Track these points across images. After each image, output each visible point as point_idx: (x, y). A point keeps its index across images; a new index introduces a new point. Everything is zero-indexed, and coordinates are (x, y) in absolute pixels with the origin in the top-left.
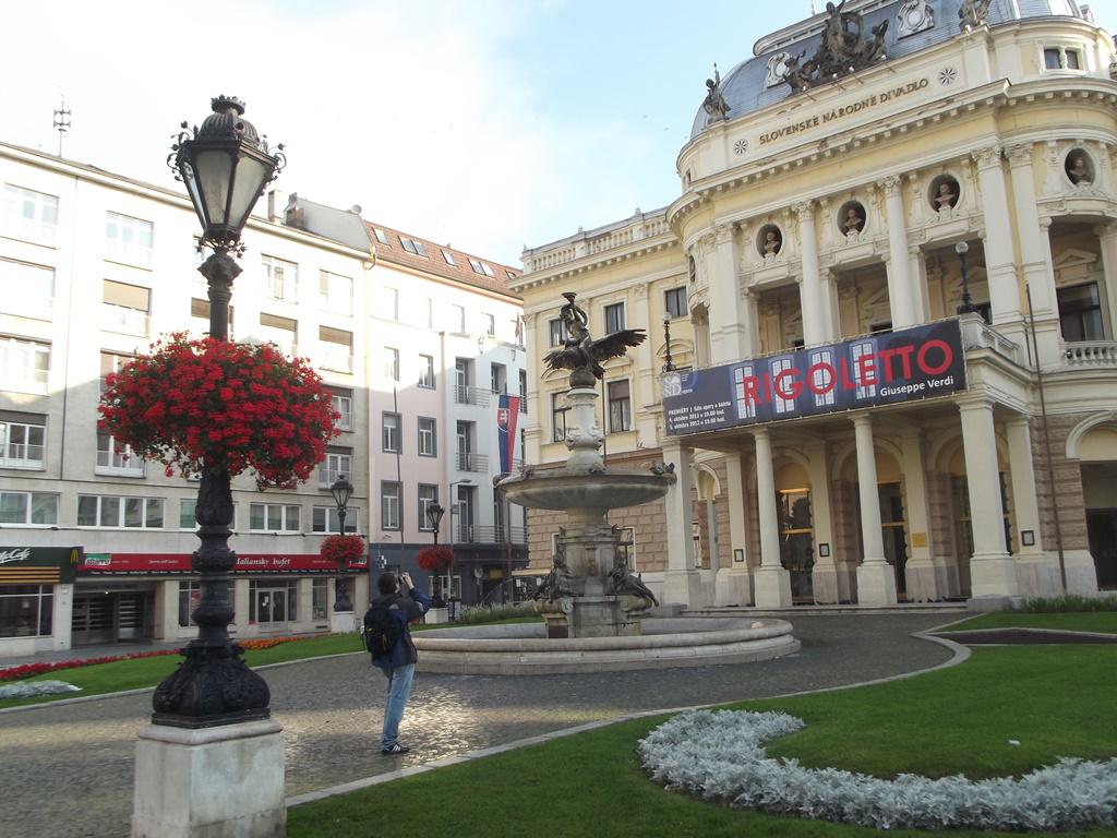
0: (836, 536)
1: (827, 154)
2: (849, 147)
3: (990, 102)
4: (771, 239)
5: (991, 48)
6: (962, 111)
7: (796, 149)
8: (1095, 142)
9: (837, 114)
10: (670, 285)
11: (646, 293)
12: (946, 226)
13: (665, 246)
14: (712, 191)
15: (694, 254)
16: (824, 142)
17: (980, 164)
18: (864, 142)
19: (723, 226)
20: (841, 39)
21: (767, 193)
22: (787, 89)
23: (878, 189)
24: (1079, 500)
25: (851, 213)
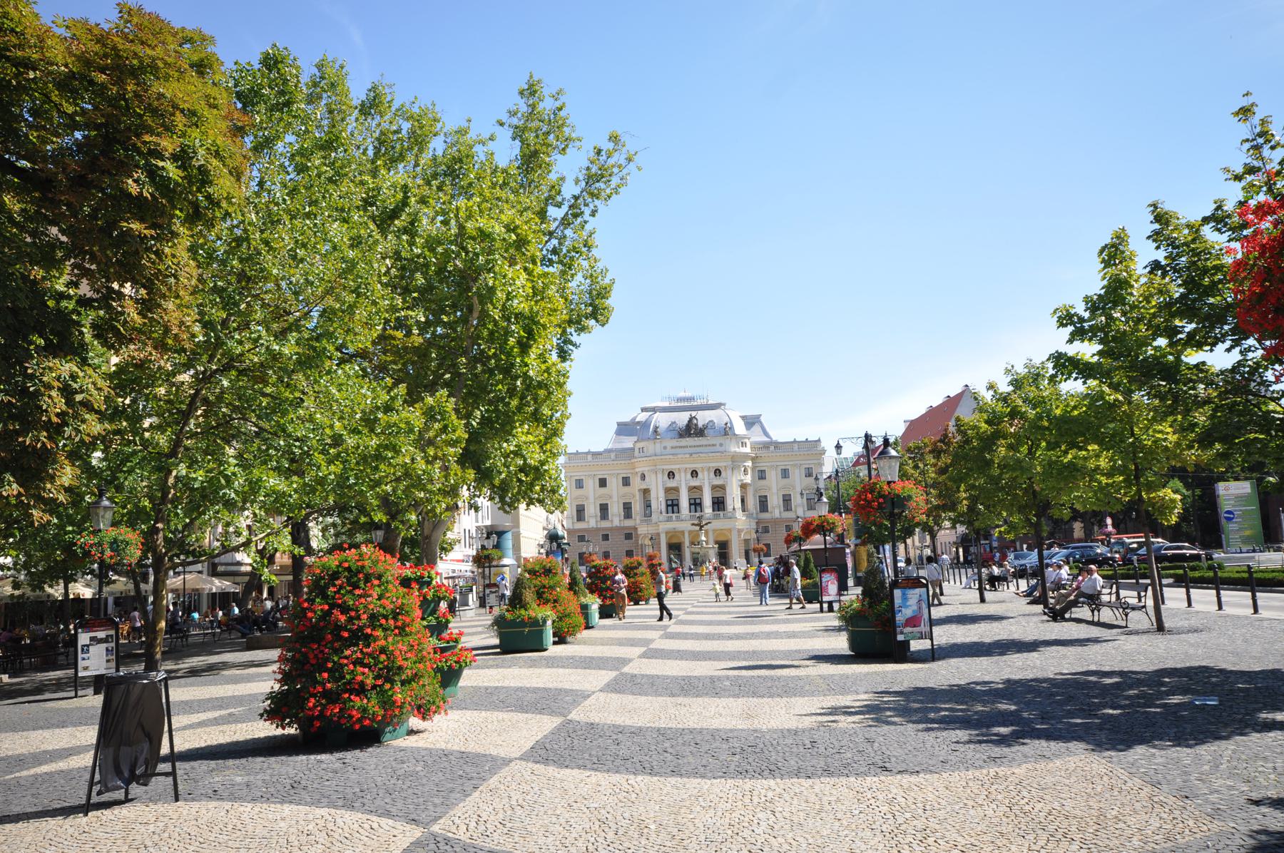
12: (718, 481)
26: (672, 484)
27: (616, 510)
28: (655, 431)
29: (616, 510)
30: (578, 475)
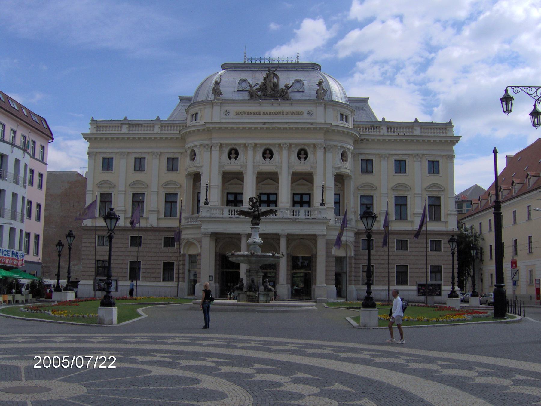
0: (215, 273)
3: (325, 129)
4: (233, 153)
5: (325, 108)
8: (349, 149)
9: (269, 113)
10: (171, 156)
11: (158, 156)
14: (213, 128)
15: (196, 149)
16: (265, 123)
17: (318, 148)
19: (216, 143)
20: (272, 85)
22: (246, 95)
23: (280, 146)
24: (334, 268)
25: (268, 152)
26: (233, 166)
27: (154, 202)
28: (216, 91)
29: (154, 202)
30: (108, 150)
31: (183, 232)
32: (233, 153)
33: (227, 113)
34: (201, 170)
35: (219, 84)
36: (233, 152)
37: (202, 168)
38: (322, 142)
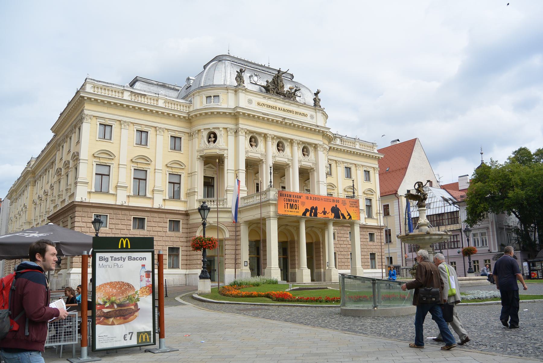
1: (283, 123)
2: (290, 124)
6: (319, 131)
7: (276, 116)
12: (307, 162)
13: (179, 116)
14: (244, 114)
15: (217, 132)
18: (294, 125)
21: (258, 125)
27: (158, 181)
31: (192, 217)
32: (253, 141)
33: (250, 102)
34: (225, 153)
35: (244, 72)
36: (253, 140)
37: (226, 151)
38: (321, 143)
